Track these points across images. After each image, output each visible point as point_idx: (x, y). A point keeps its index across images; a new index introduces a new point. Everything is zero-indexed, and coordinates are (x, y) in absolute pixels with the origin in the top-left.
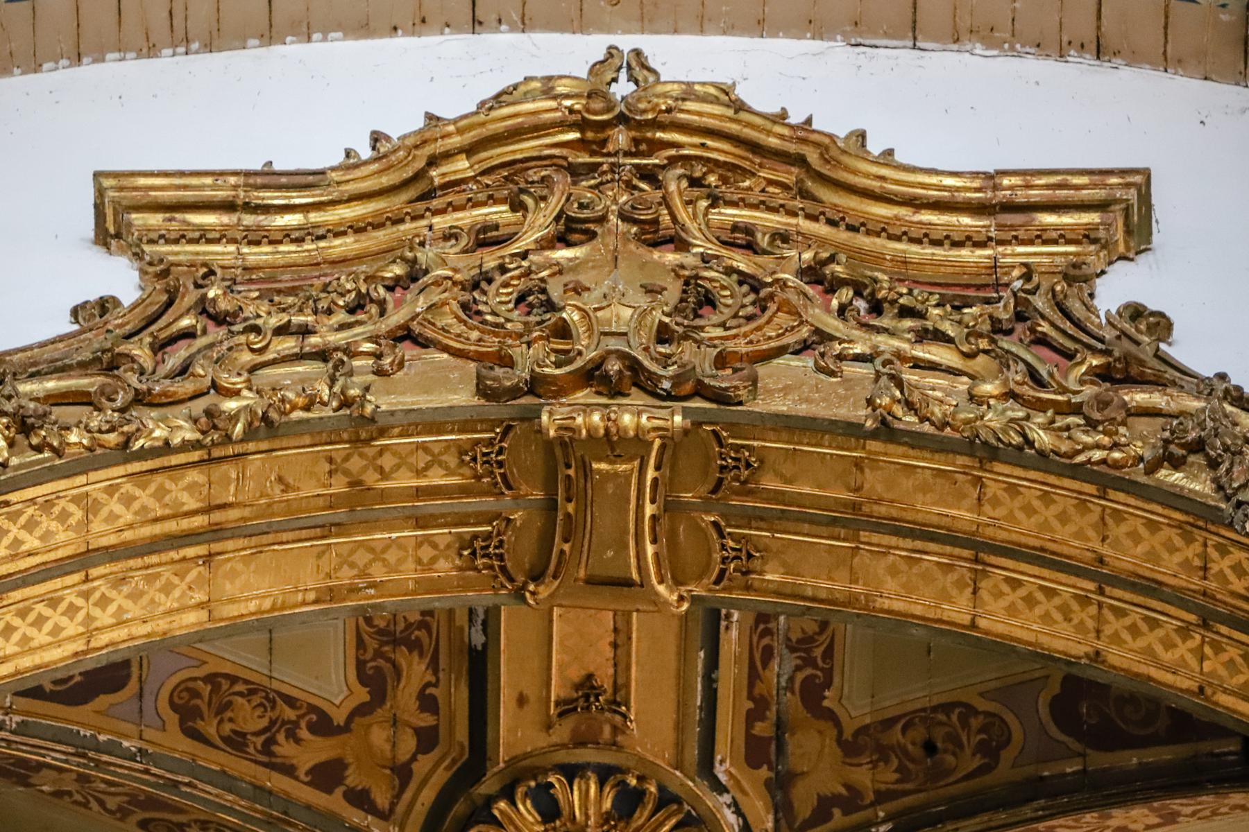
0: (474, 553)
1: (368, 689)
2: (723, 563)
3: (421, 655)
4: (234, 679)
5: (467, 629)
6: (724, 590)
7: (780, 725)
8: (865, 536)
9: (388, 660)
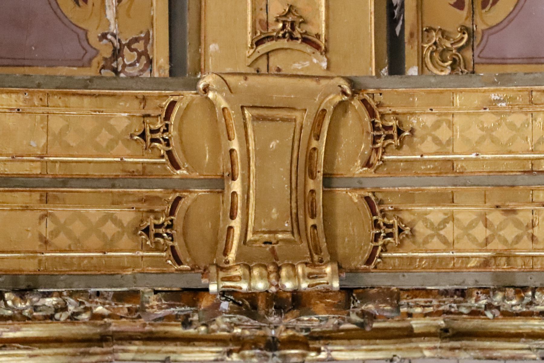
0: (400, 132)
2: (167, 126)
6: (167, 96)
8: (36, 168)
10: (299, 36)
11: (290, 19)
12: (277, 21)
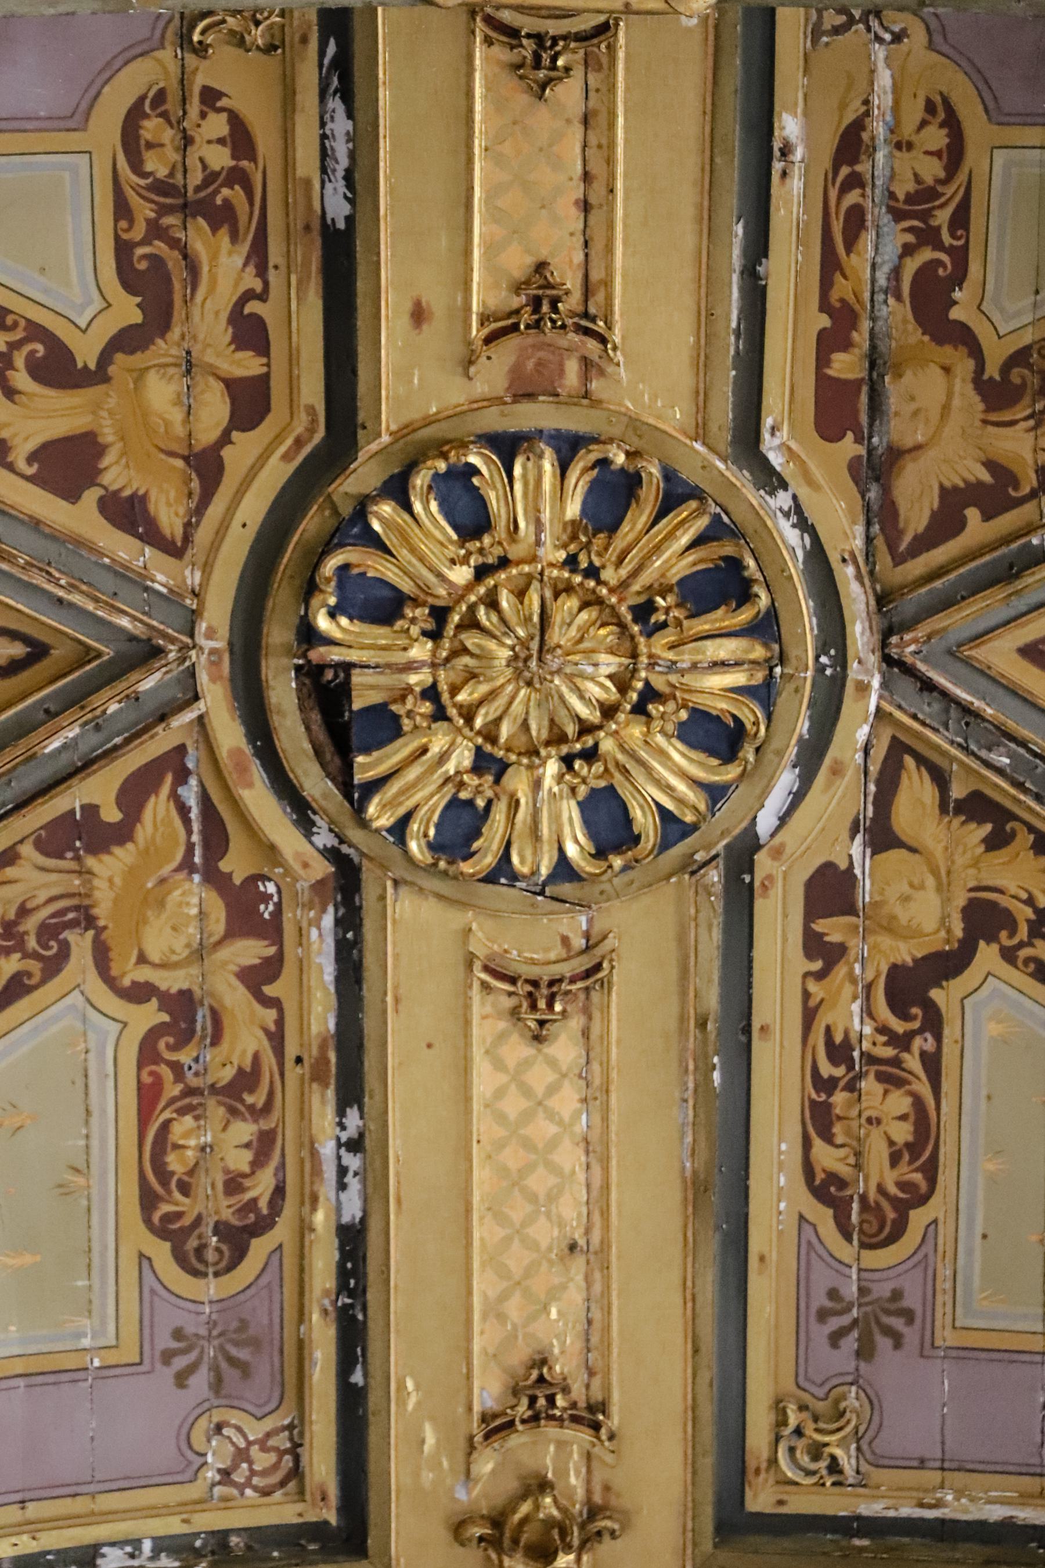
1: (139, 299)
3: (235, 237)
5: (317, 186)
7: (874, 357)
9: (174, 243)
10: (525, 41)
11: (542, 74)
12: (567, 69)
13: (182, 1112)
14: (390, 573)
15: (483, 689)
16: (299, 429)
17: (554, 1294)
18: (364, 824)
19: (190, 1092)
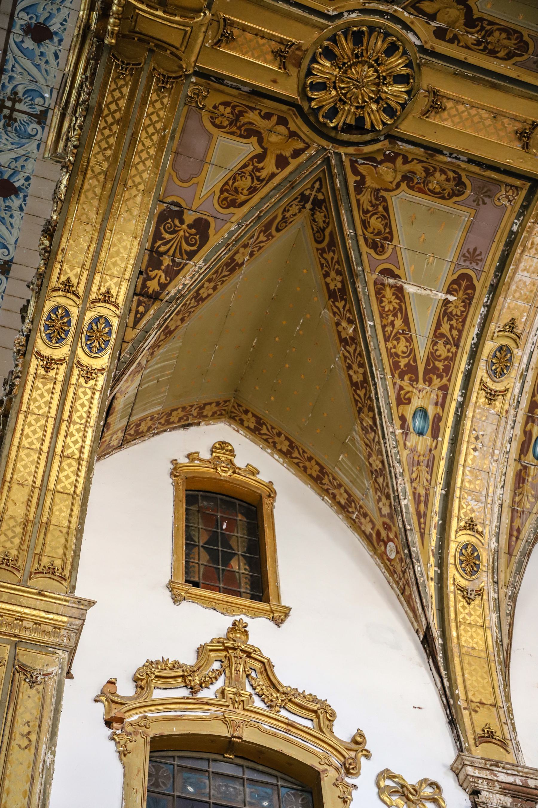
3: (247, 112)
4: (226, 183)
9: (243, 125)
13: (427, 185)
14: (327, 107)
15: (360, 97)
16: (291, 113)
17: (503, 124)
18: (380, 131)
19: (424, 182)
